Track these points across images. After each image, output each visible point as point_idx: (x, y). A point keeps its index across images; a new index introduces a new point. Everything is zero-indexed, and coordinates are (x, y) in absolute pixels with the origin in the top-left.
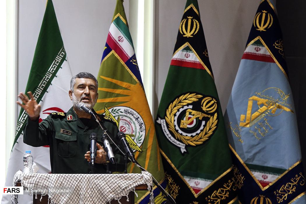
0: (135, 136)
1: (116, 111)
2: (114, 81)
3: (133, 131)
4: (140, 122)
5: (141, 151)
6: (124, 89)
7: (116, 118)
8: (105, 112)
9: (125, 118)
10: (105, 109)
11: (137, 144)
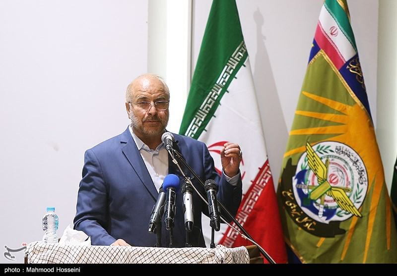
0: (352, 191)
3: (349, 183)
4: (360, 168)
5: (360, 215)
11: (355, 204)
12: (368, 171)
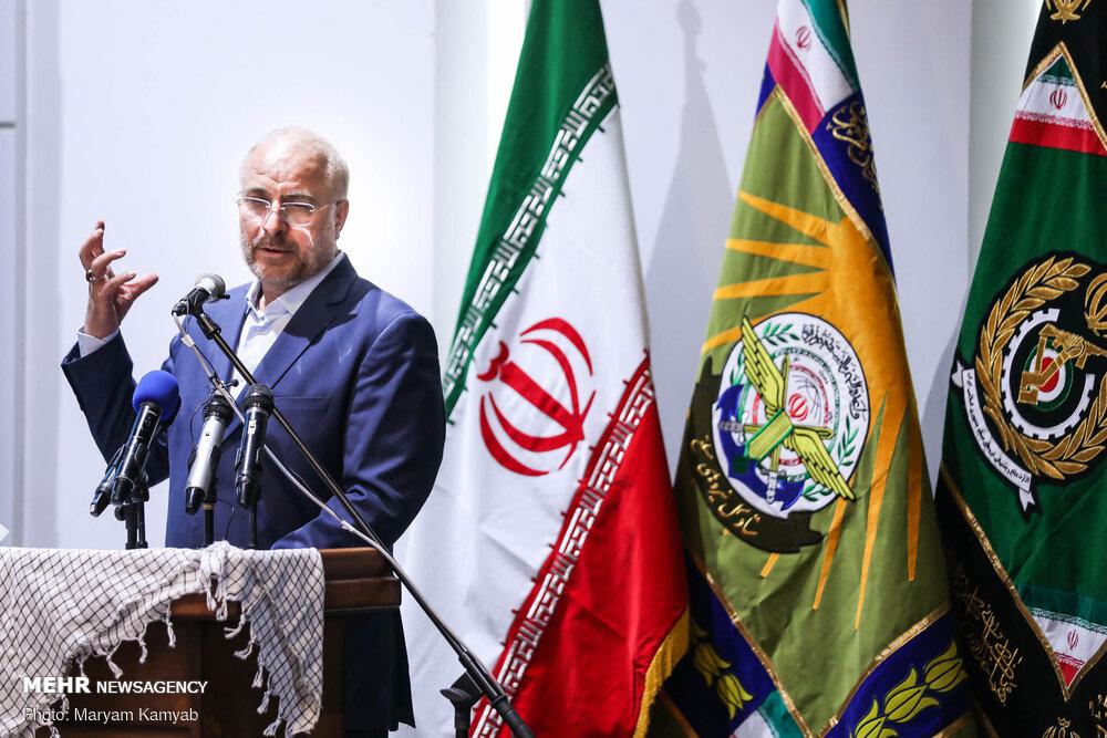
0: (835, 435)
1: (777, 332)
2: (776, 210)
6: (806, 243)
7: (779, 361)
8: (743, 336)
9: (805, 361)
10: (743, 324)
11: (842, 468)
12: (872, 385)
